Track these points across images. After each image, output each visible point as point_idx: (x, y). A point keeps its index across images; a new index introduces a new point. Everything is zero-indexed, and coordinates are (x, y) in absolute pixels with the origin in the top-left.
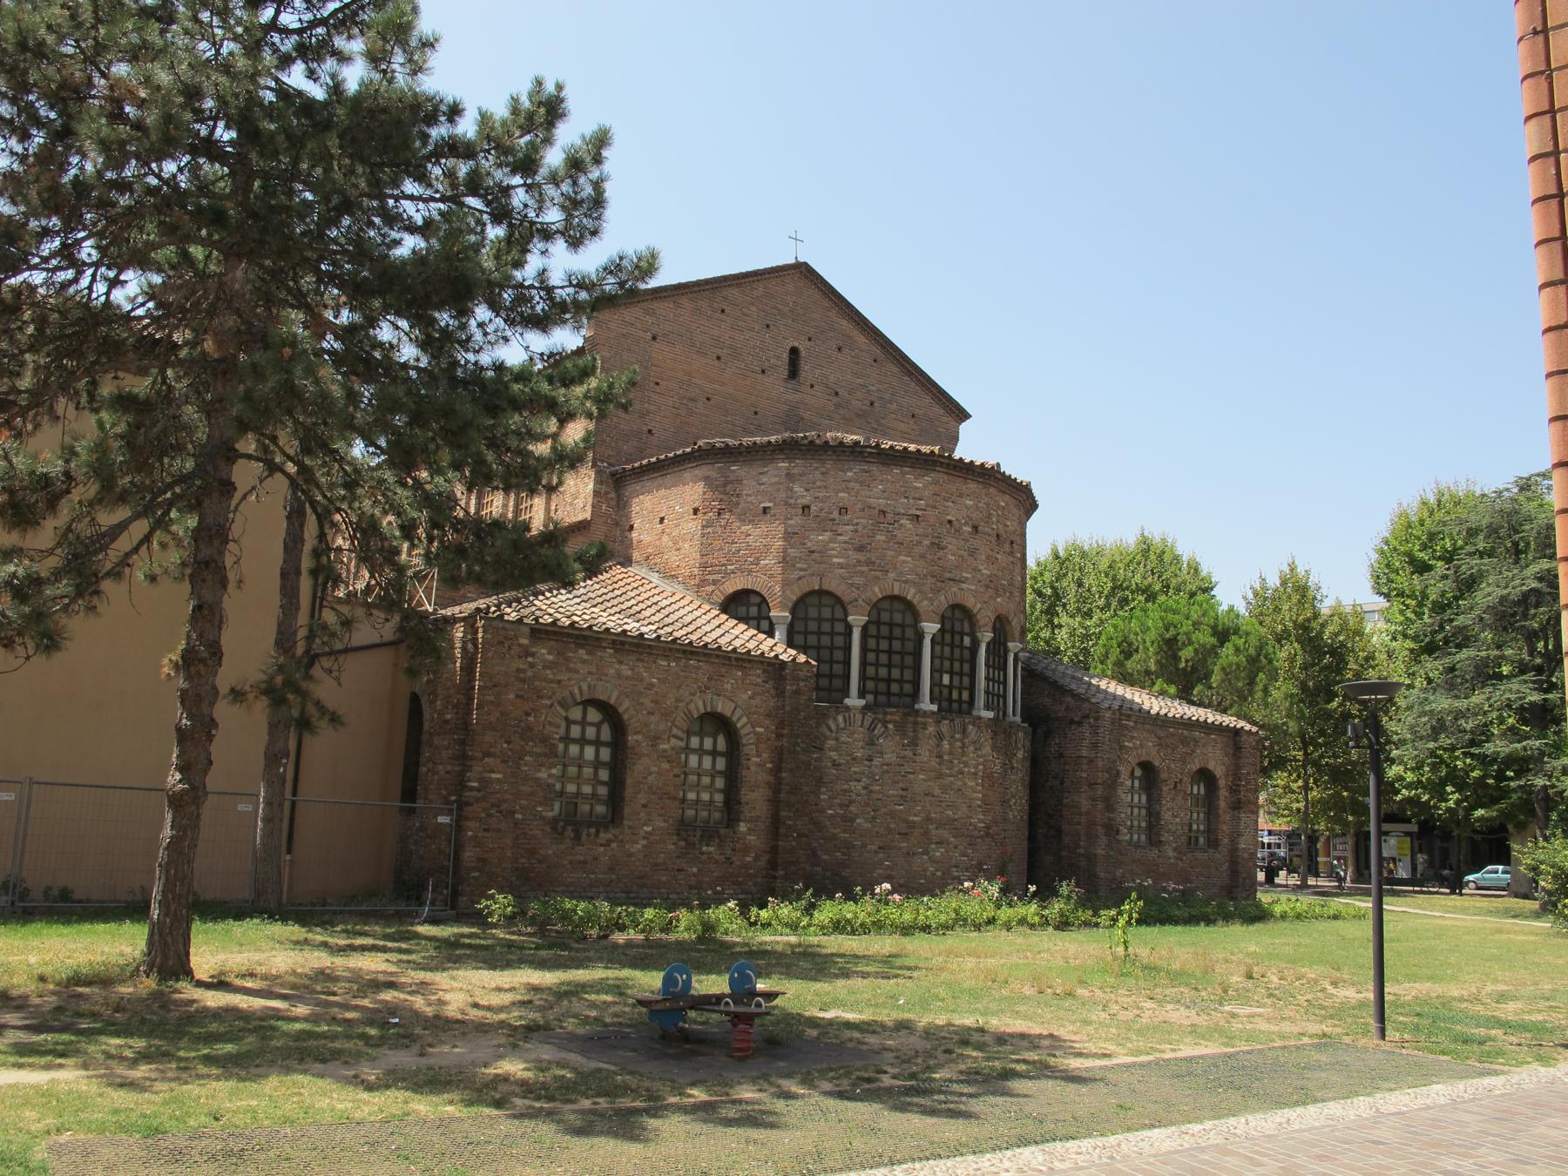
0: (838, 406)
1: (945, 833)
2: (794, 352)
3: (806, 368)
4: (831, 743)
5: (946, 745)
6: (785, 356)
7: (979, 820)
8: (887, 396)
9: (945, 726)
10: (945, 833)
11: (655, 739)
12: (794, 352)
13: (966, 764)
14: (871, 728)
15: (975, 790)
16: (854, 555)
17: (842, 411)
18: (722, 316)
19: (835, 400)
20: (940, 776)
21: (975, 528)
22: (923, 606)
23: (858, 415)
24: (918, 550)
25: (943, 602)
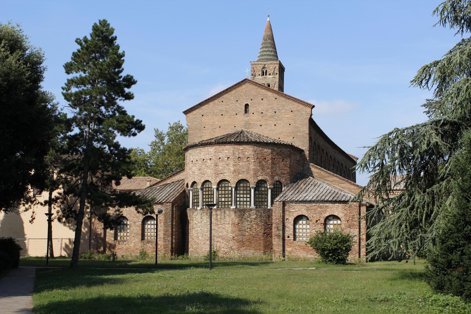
0: (262, 117)
1: (220, 240)
2: (247, 106)
3: (250, 109)
4: (195, 219)
5: (219, 217)
6: (244, 108)
7: (231, 235)
8: (281, 108)
9: (218, 212)
10: (220, 240)
11: (135, 223)
12: (247, 106)
13: (226, 221)
14: (201, 214)
15: (229, 228)
16: (198, 172)
17: (264, 118)
18: (223, 103)
19: (262, 115)
20: (218, 225)
21: (228, 158)
22: (213, 182)
23: (270, 117)
24: (212, 167)
25: (218, 180)
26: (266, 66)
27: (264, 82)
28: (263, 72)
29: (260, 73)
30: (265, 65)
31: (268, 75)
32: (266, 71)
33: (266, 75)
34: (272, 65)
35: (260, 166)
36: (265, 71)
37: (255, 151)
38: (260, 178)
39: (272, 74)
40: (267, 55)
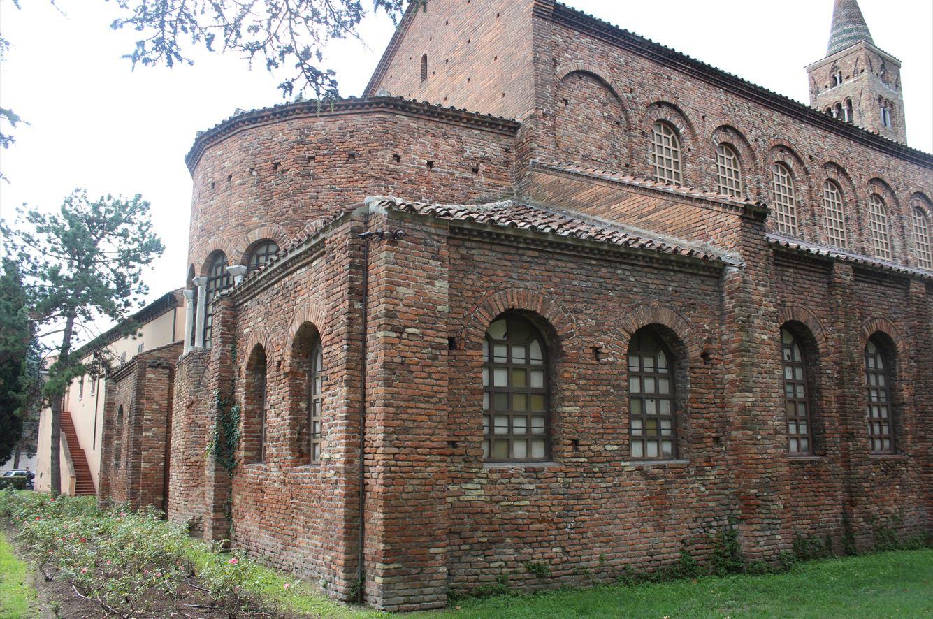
23: (460, 63)
26: (838, 63)
27: (837, 98)
28: (836, 79)
29: (828, 83)
30: (835, 62)
31: (843, 80)
32: (840, 73)
33: (841, 82)
34: (850, 57)
35: (258, 196)
36: (837, 76)
37: (246, 149)
38: (256, 235)
39: (851, 75)
40: (842, 41)
